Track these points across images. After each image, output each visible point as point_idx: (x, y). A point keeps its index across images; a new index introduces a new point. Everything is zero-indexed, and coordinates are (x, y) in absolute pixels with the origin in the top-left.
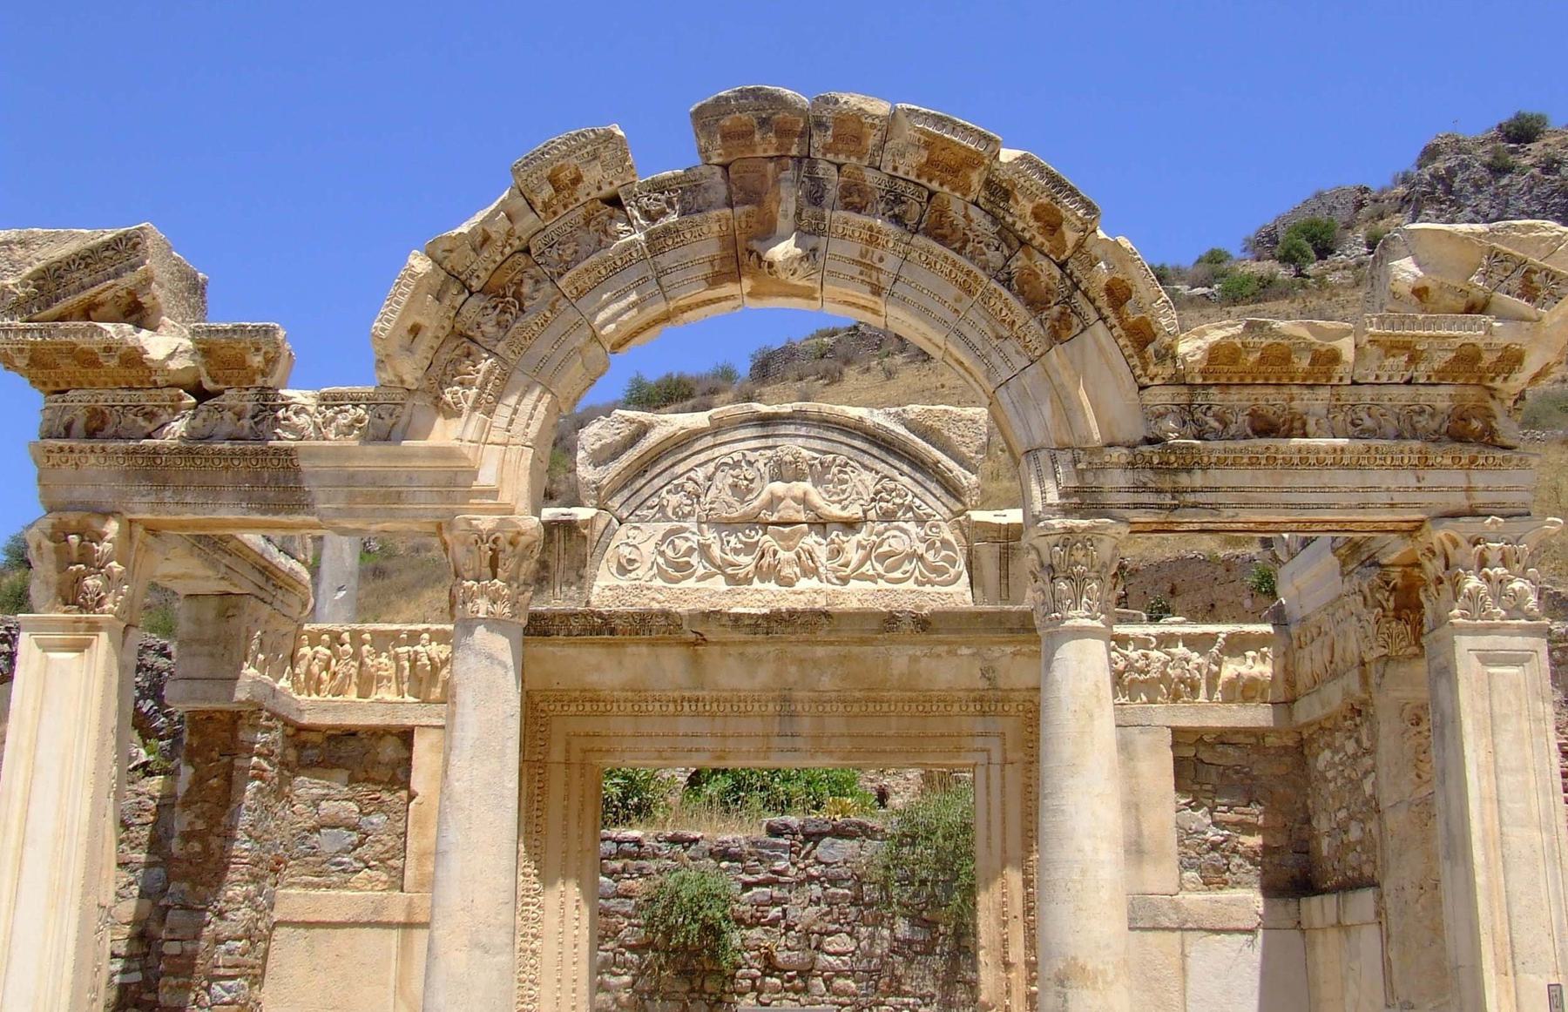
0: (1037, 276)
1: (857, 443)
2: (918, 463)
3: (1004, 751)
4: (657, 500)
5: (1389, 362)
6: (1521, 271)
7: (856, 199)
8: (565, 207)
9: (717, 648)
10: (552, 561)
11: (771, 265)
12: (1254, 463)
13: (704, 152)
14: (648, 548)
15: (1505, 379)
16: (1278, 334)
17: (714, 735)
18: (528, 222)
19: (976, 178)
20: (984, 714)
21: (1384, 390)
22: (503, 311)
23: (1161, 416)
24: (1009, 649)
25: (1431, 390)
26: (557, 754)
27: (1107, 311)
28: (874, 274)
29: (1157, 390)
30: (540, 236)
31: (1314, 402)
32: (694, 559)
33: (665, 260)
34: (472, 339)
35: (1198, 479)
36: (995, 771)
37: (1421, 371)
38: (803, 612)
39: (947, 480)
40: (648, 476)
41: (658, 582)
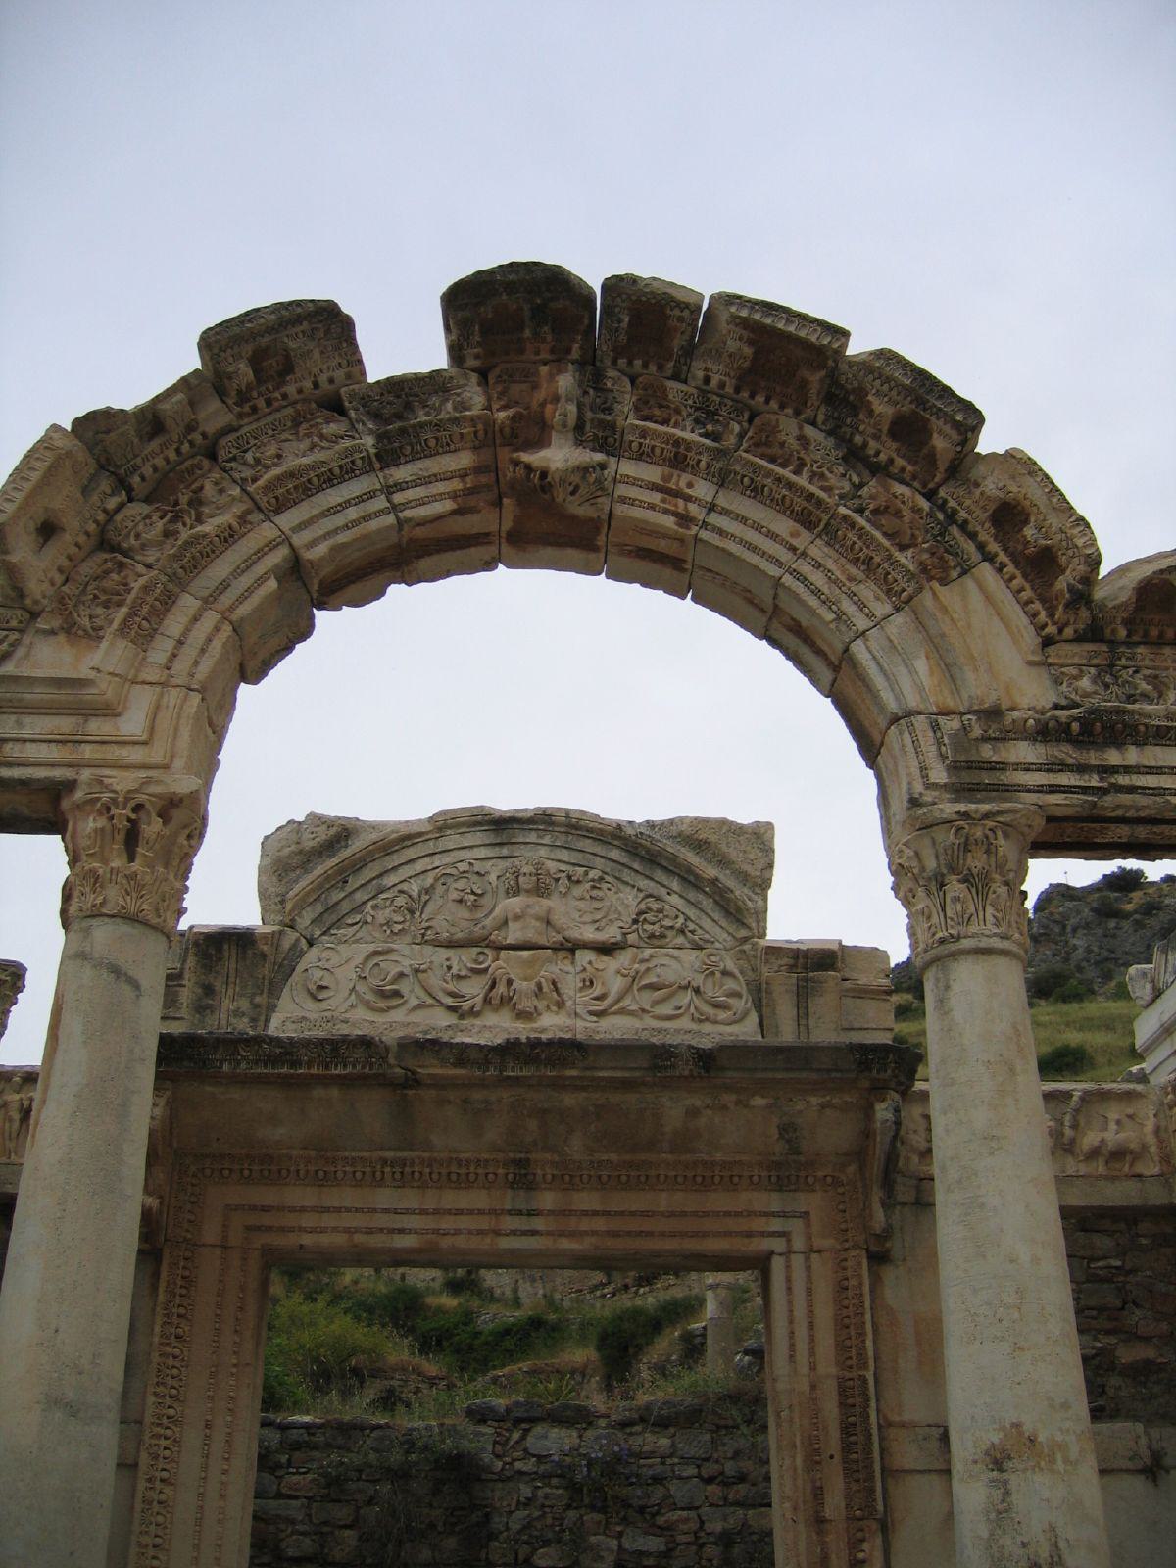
0: (898, 514)
1: (615, 854)
2: (690, 879)
3: (809, 1237)
4: (358, 918)
7: (657, 412)
8: (269, 402)
9: (433, 1092)
10: (218, 985)
11: (544, 474)
13: (455, 352)
14: (347, 975)
17: (423, 1212)
18: (214, 415)
19: (815, 379)
20: (781, 1185)
22: (176, 519)
24: (814, 1100)
26: (211, 1233)
27: (993, 547)
28: (681, 502)
30: (232, 437)
32: (404, 987)
33: (402, 473)
34: (125, 553)
35: (1132, 756)
36: (797, 1261)
38: (550, 1043)
39: (729, 900)
40: (349, 888)
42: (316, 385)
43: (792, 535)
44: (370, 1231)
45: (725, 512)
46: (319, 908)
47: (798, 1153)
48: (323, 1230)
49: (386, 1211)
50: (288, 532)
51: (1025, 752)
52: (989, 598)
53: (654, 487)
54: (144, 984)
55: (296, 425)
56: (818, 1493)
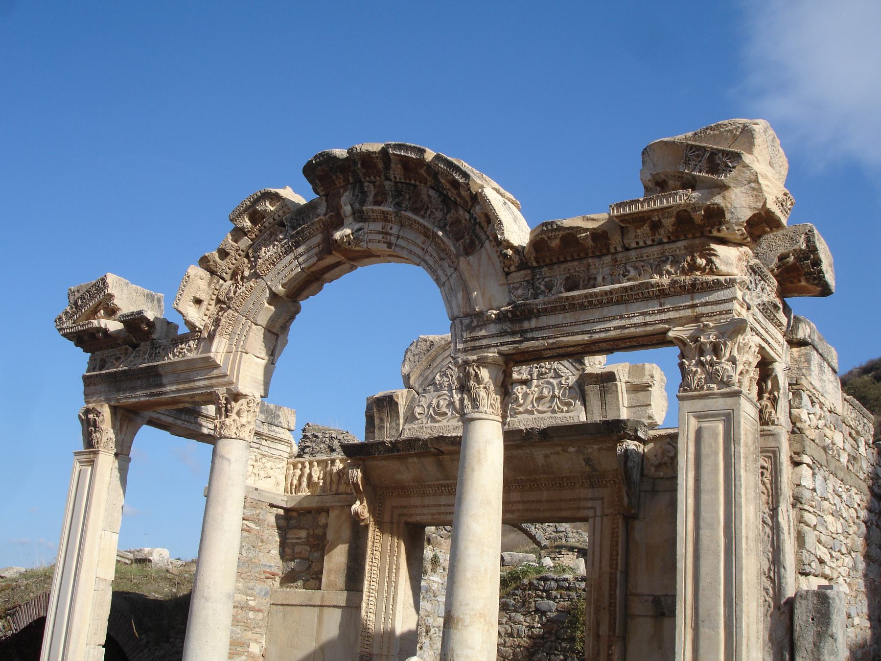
0: (460, 221)
3: (603, 508)
5: (639, 232)
6: (707, 155)
7: (379, 198)
11: (336, 241)
12: (563, 309)
15: (719, 231)
16: (560, 228)
19: (423, 172)
21: (643, 251)
23: (517, 289)
24: (596, 447)
25: (673, 246)
29: (514, 275)
31: (601, 267)
34: (224, 303)
35: (533, 323)
36: (598, 519)
37: (662, 235)
41: (430, 424)
42: (274, 219)
43: (423, 243)
44: (439, 514)
45: (403, 238)
46: (421, 379)
47: (596, 470)
48: (424, 514)
49: (445, 505)
50: (269, 283)
51: (493, 329)
52: (489, 257)
53: (380, 232)
54: (232, 460)
55: (271, 236)
56: (598, 624)
